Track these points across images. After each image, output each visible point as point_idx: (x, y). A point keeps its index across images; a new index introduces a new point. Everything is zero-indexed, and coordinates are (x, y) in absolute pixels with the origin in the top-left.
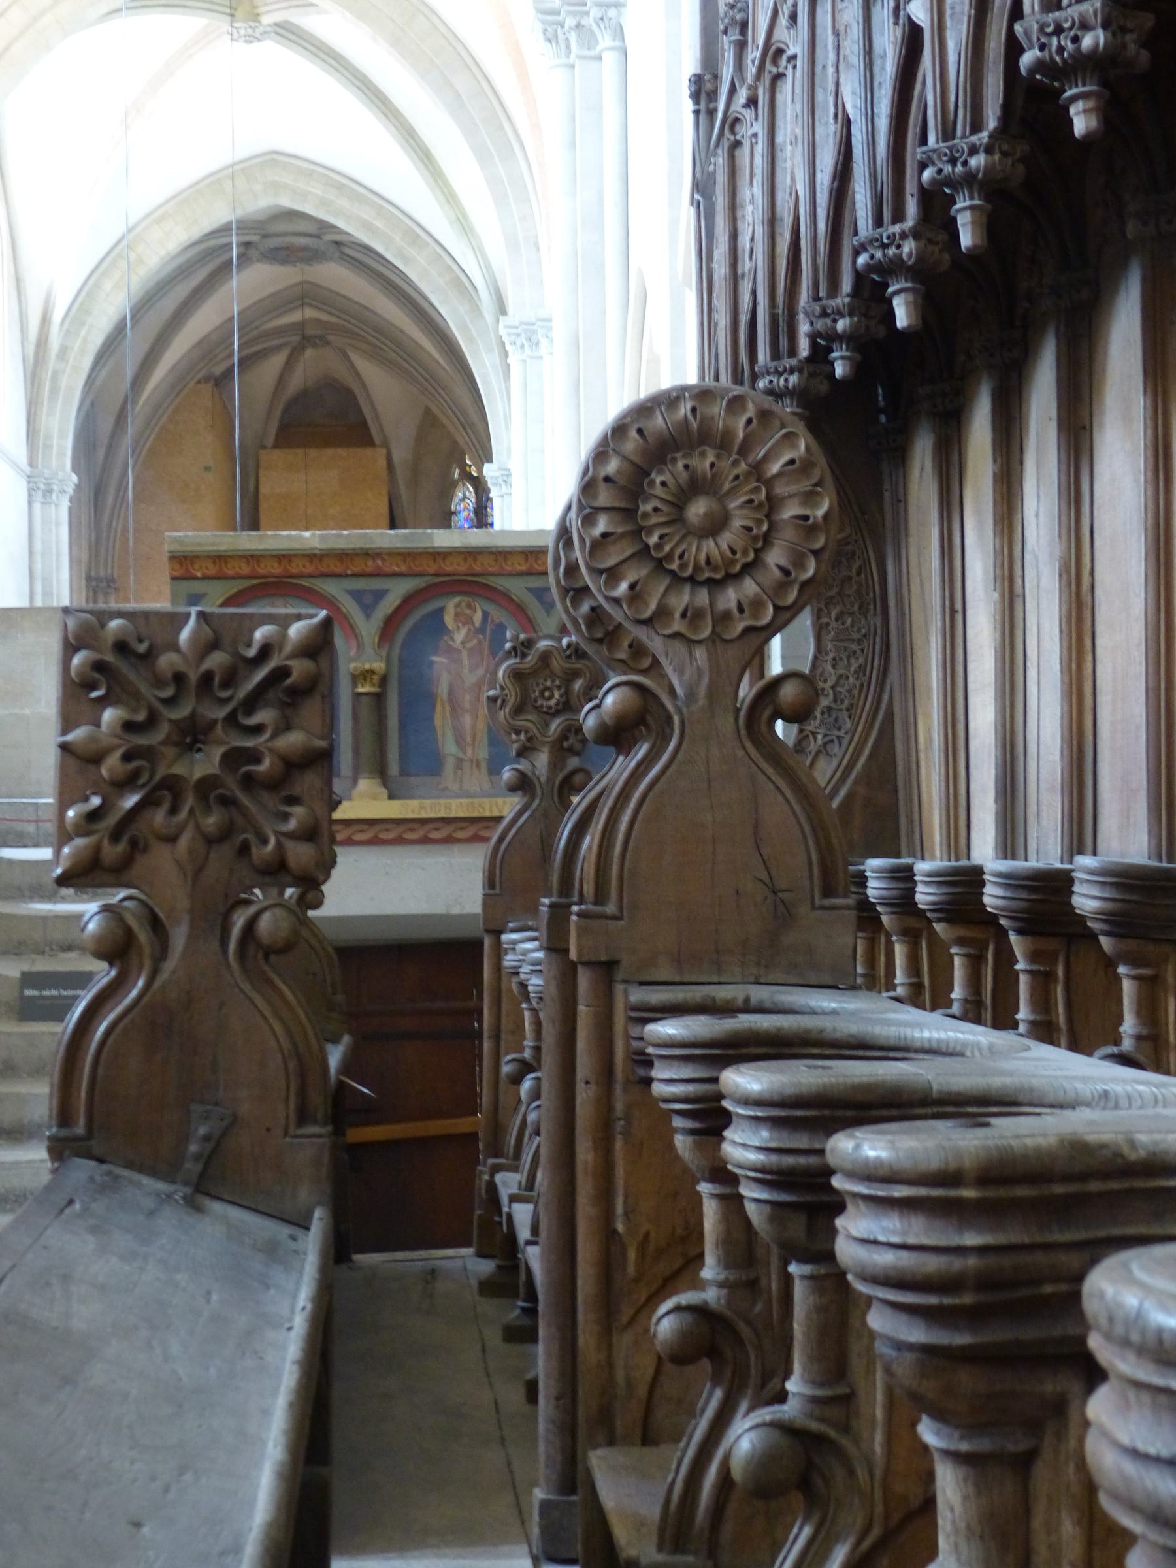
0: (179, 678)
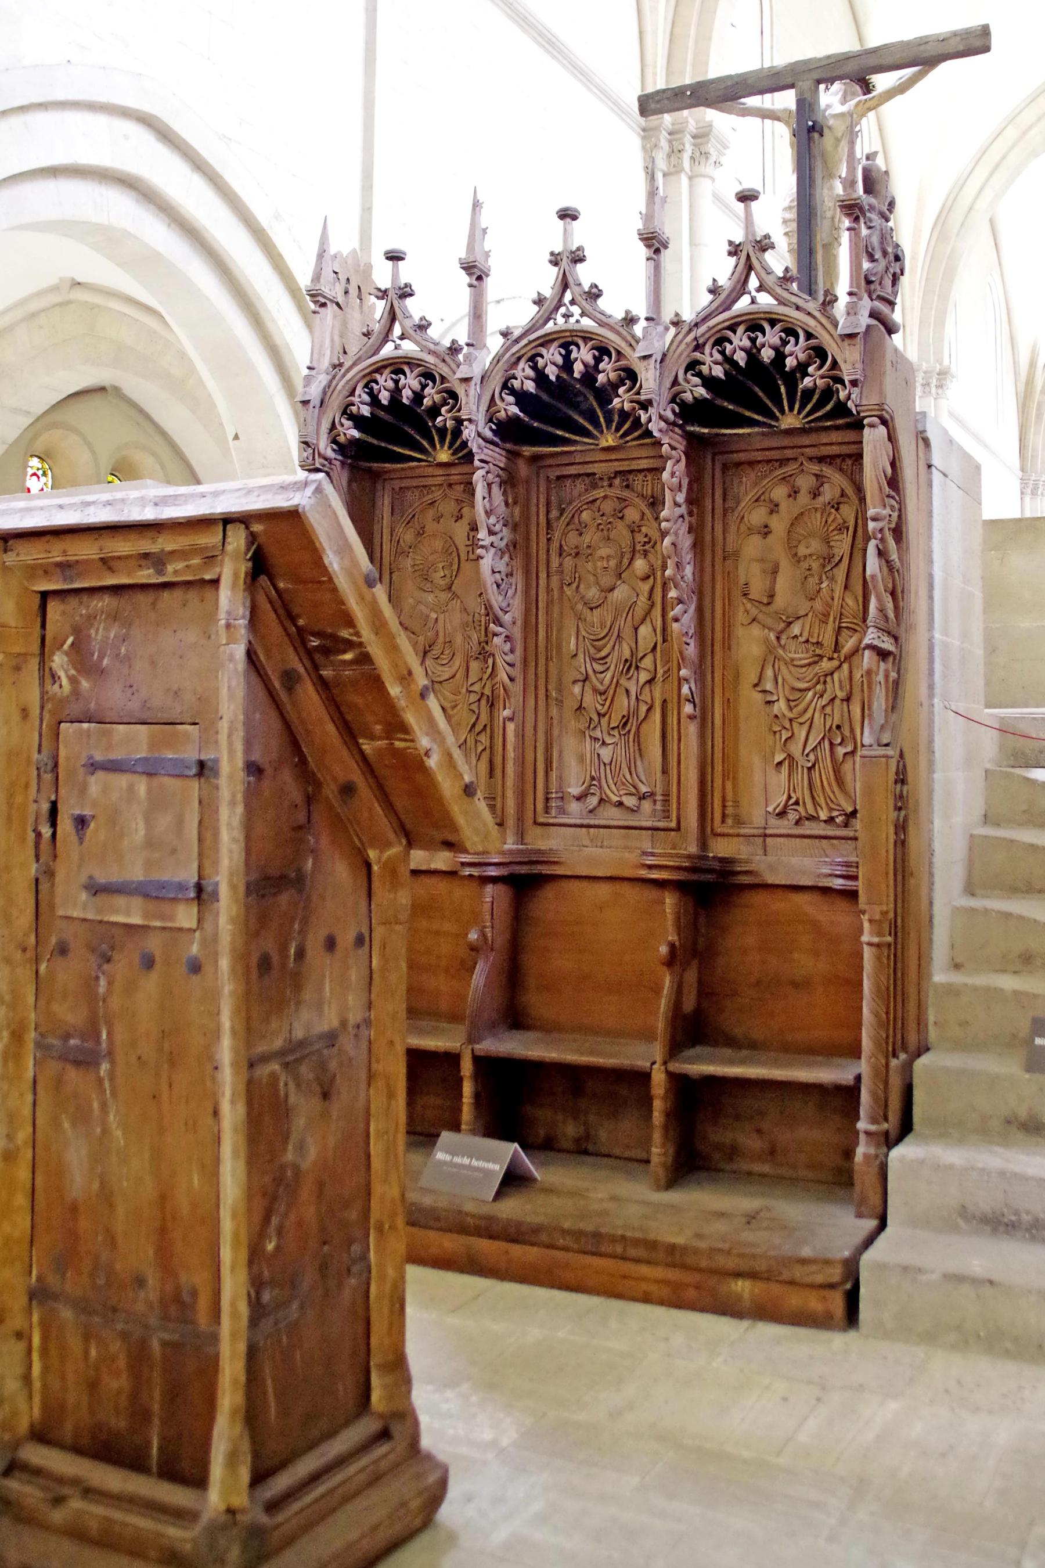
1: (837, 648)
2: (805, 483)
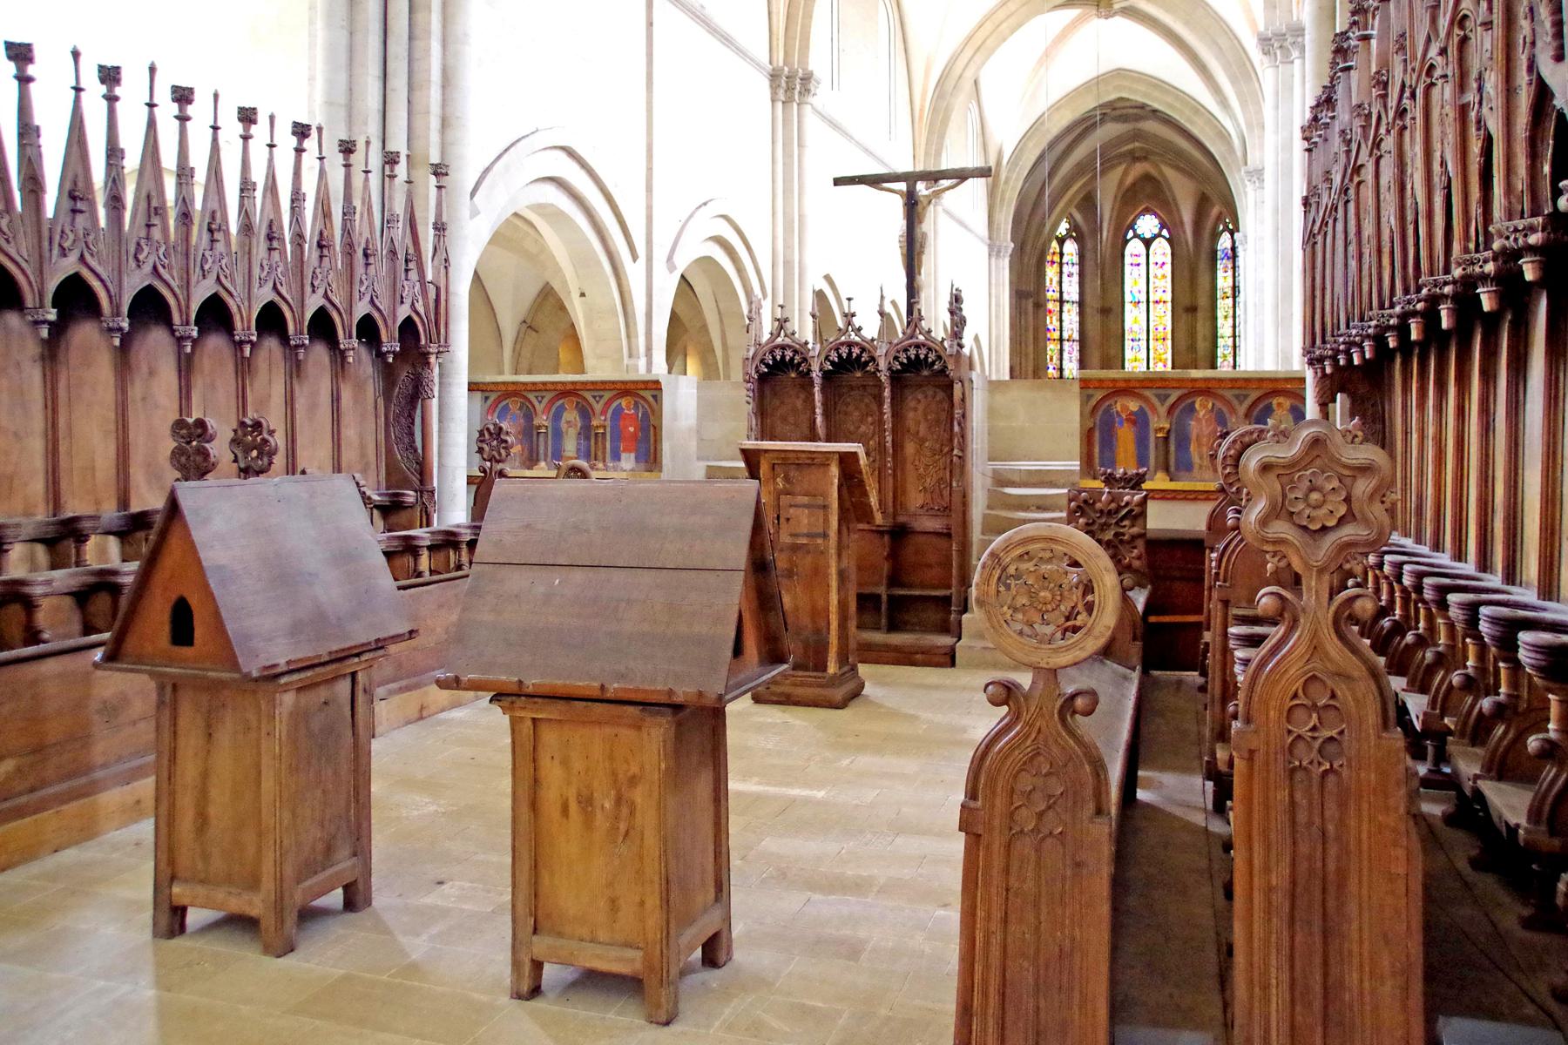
0: (1101, 511)
1: (941, 451)
2: (930, 393)
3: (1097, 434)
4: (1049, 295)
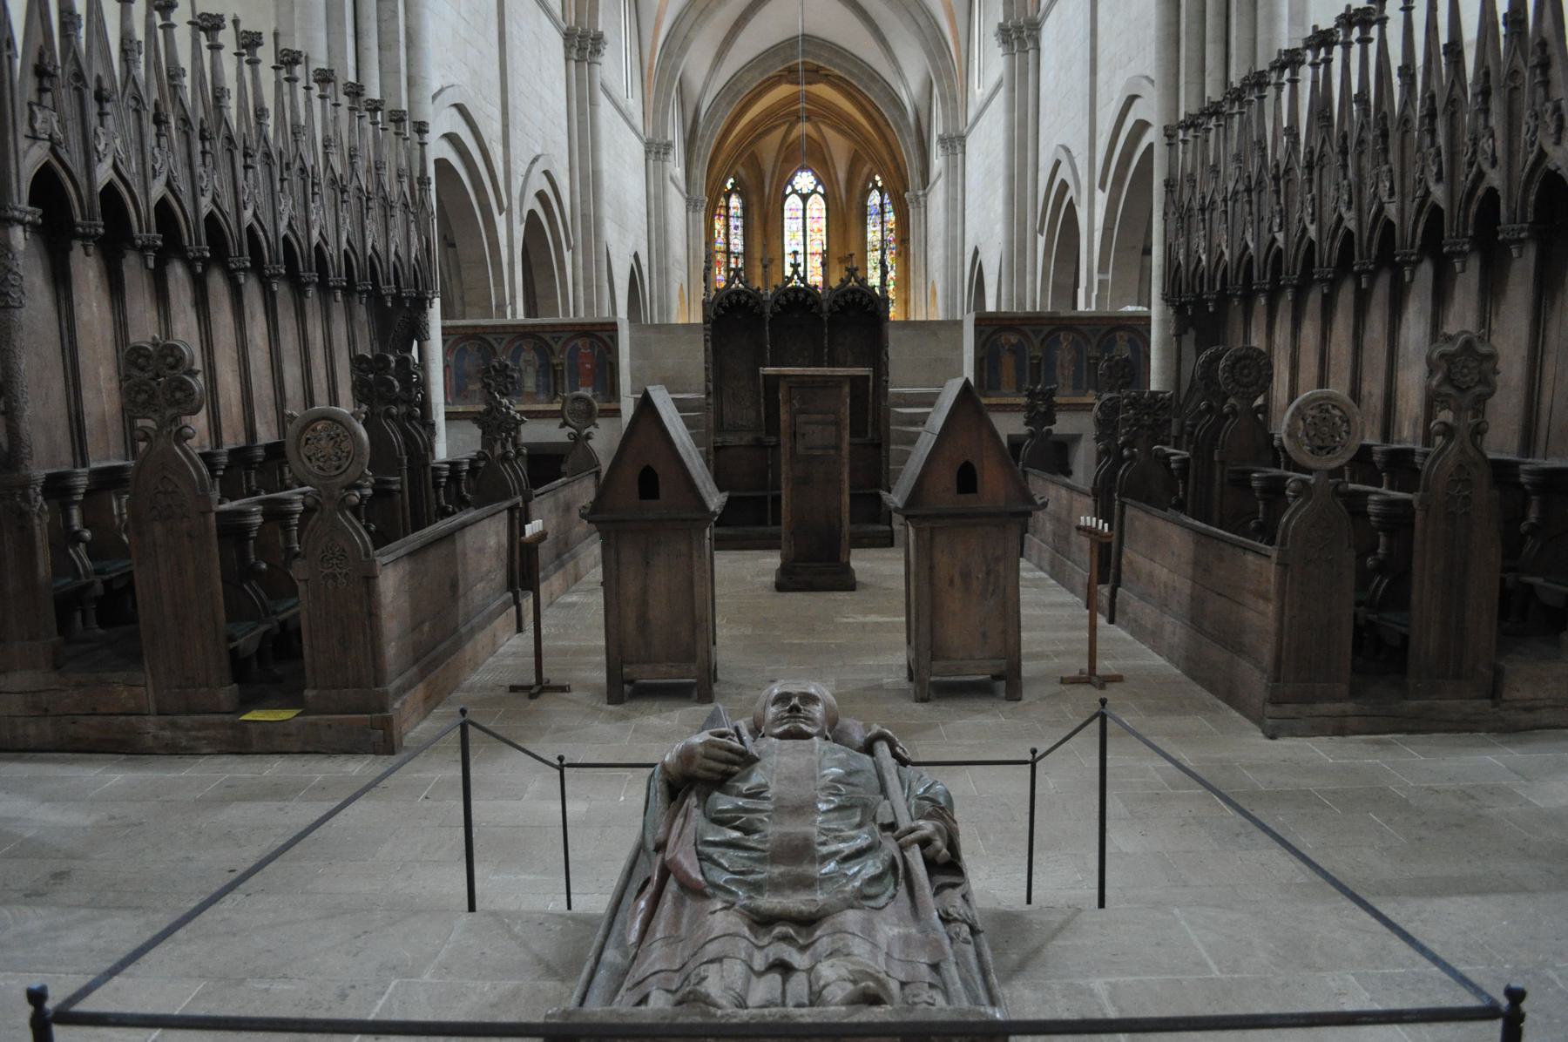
3: (986, 361)
4: (718, 245)
